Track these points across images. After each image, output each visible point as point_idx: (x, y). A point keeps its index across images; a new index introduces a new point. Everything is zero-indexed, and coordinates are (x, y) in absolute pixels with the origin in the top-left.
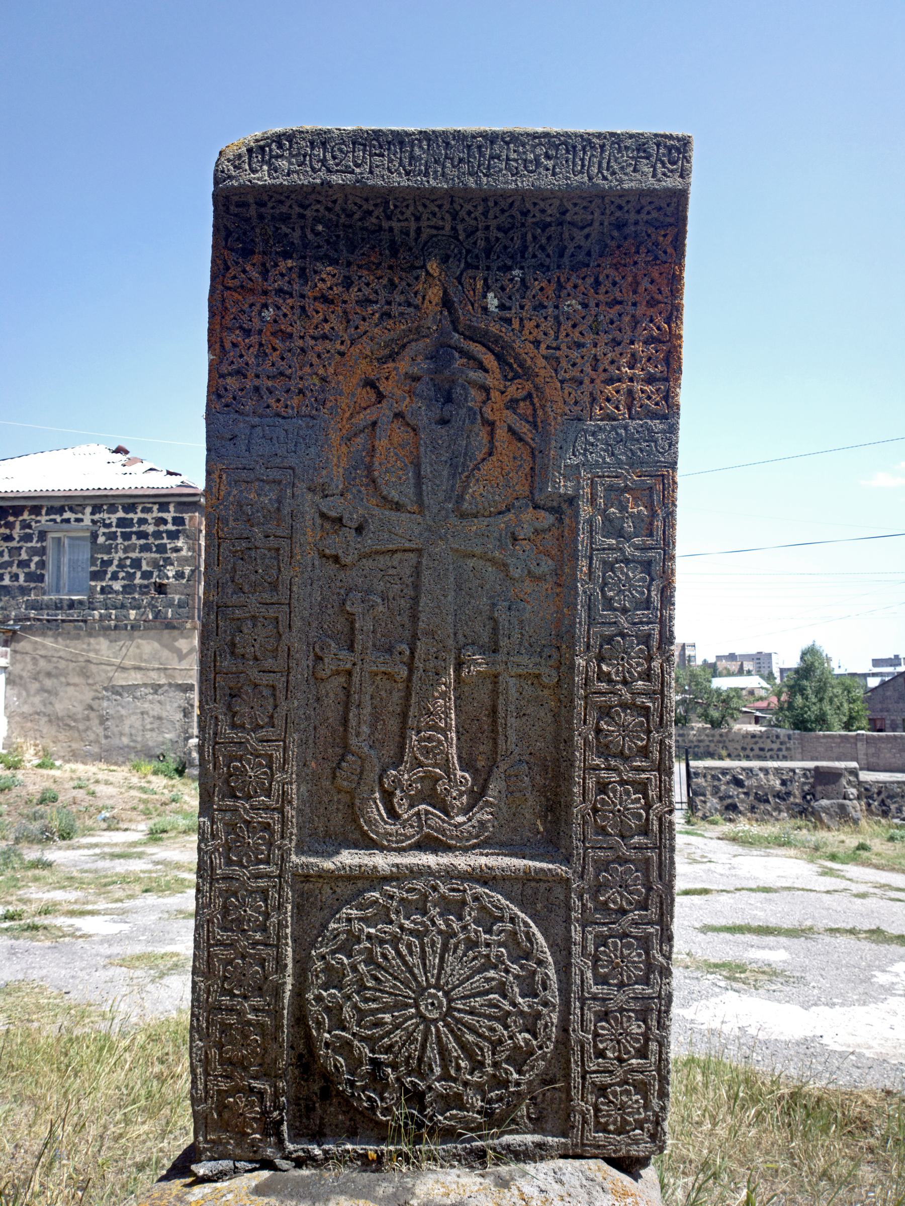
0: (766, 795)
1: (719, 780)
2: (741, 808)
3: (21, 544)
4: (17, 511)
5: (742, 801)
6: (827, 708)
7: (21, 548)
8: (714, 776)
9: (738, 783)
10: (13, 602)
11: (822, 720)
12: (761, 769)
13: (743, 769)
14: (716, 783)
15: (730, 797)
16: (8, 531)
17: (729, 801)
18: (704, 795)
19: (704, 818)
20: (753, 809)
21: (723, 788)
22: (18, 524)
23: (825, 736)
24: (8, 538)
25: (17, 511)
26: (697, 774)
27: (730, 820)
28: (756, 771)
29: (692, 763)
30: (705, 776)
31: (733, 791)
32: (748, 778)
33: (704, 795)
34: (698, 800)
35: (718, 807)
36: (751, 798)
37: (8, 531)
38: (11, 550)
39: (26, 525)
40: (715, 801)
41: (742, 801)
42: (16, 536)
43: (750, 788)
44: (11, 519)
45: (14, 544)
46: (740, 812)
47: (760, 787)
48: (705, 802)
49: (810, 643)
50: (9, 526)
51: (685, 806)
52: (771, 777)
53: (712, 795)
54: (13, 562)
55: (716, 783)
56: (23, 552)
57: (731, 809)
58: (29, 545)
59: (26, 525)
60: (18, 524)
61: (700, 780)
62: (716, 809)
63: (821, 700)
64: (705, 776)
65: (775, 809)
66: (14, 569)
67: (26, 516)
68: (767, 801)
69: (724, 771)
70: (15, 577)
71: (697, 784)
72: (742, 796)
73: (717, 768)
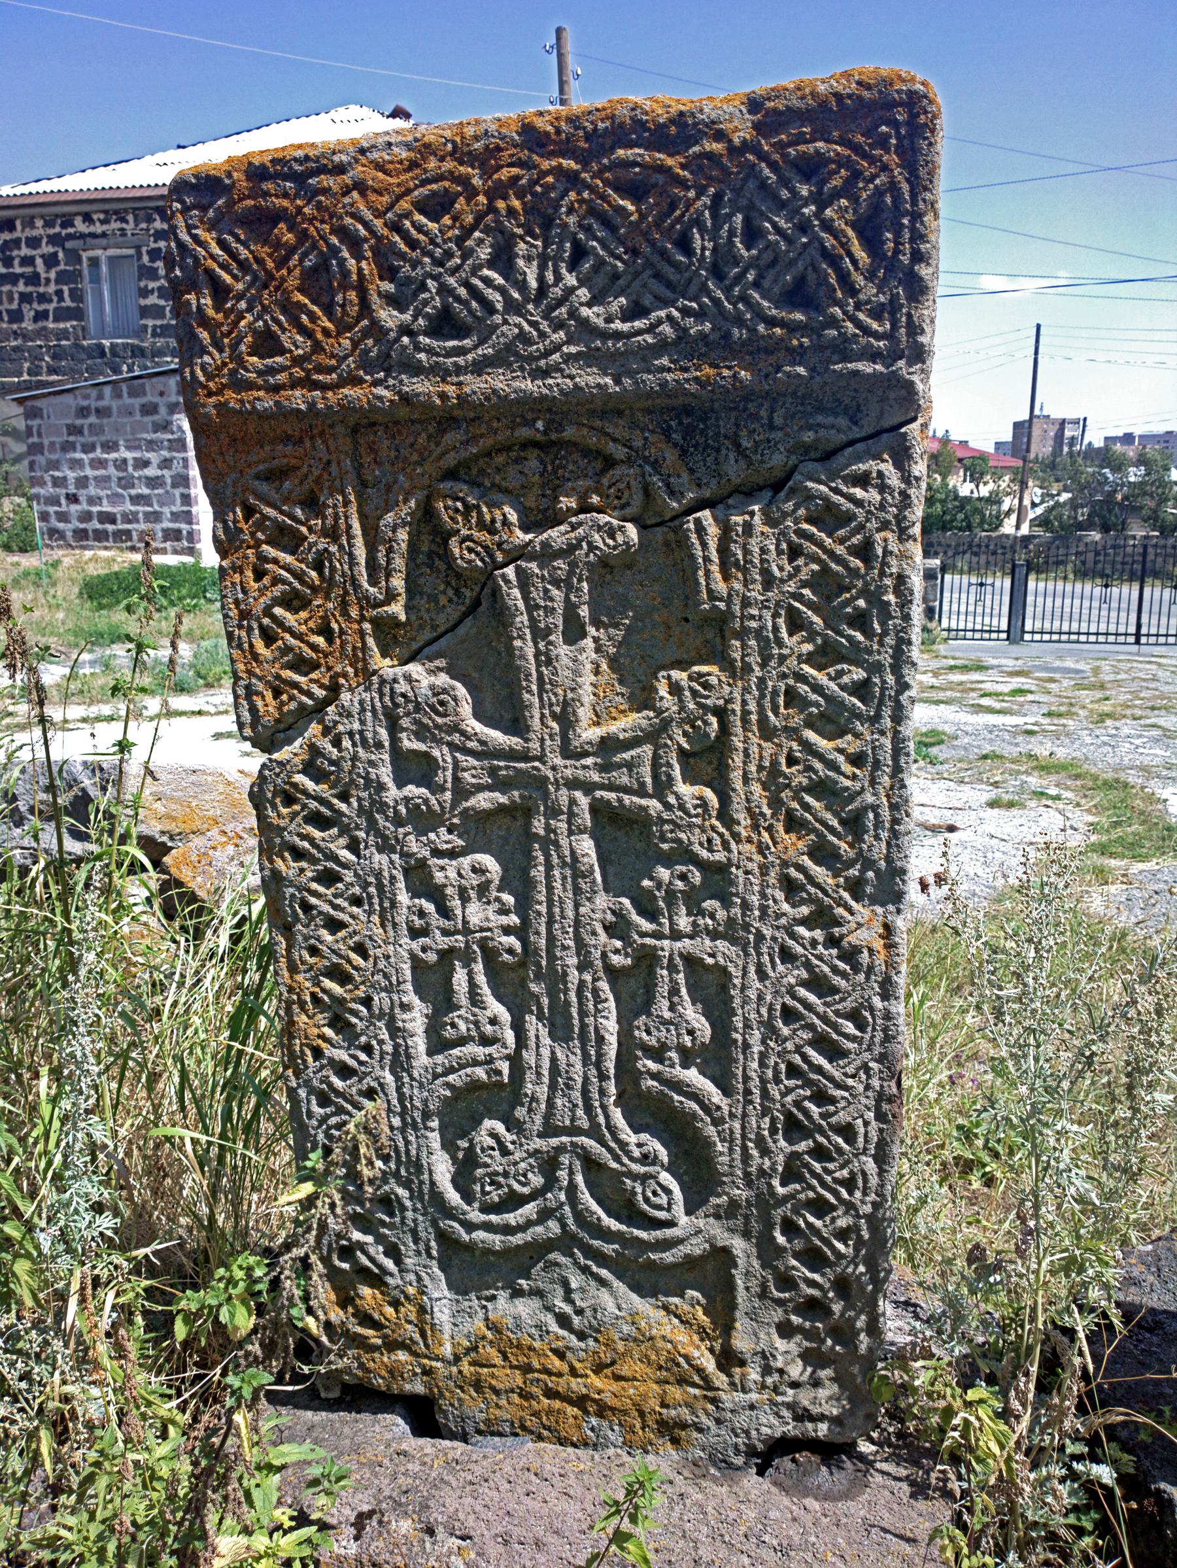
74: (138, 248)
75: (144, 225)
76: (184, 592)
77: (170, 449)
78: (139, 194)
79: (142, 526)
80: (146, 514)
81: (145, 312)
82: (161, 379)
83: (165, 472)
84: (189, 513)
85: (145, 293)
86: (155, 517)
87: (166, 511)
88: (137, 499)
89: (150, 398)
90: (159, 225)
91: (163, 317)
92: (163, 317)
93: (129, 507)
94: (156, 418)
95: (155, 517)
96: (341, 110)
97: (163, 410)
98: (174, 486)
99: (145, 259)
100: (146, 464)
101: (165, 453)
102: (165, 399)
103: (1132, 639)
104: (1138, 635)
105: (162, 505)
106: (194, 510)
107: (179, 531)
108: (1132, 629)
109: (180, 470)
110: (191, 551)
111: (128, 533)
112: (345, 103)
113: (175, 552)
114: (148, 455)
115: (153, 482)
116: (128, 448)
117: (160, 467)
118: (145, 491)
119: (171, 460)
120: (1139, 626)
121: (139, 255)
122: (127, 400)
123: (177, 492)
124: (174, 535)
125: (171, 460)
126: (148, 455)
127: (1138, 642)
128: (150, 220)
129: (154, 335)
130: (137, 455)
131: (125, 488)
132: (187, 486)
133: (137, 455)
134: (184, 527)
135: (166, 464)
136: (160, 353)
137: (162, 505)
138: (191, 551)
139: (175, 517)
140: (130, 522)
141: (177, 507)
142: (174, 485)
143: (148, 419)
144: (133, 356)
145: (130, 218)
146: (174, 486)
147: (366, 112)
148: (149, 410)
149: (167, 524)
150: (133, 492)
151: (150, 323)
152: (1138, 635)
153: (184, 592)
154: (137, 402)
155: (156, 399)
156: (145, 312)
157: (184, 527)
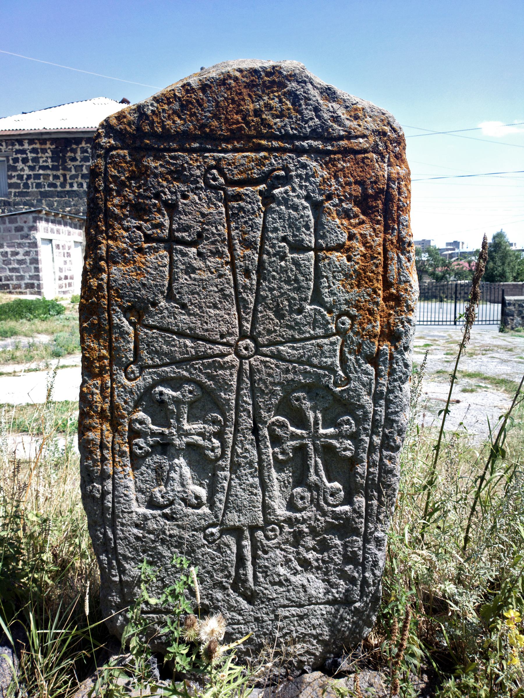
3: (82, 163)
4: (78, 141)
6: (507, 269)
7: (82, 166)
10: (81, 201)
11: (503, 276)
16: (73, 155)
18: (513, 316)
19: (512, 329)
22: (79, 150)
23: (503, 285)
24: (74, 159)
25: (78, 141)
26: (510, 304)
29: (507, 298)
33: (513, 316)
34: (509, 319)
37: (73, 155)
38: (76, 167)
39: (84, 151)
40: (519, 319)
42: (78, 158)
44: (74, 146)
45: (78, 163)
49: (499, 231)
50: (74, 151)
51: (499, 322)
53: (518, 316)
54: (78, 175)
56: (84, 168)
58: (88, 164)
59: (84, 151)
60: (79, 150)
61: (512, 308)
63: (503, 264)
64: (514, 305)
66: (80, 179)
67: (83, 145)
70: (80, 185)
74: (7, 157)
75: (10, 147)
76: (41, 311)
77: (29, 247)
78: (8, 133)
79: (15, 282)
80: (17, 277)
81: (11, 186)
82: (25, 215)
83: (27, 257)
84: (38, 276)
85: (10, 177)
86: (22, 278)
87: (27, 275)
88: (12, 270)
89: (20, 224)
90: (17, 147)
91: (20, 188)
92: (20, 188)
93: (8, 273)
94: (22, 233)
95: (22, 278)
96: (97, 99)
97: (26, 230)
98: (31, 263)
99: (11, 162)
100: (17, 254)
101: (27, 249)
102: (27, 224)
103: (453, 323)
104: (455, 322)
105: (25, 272)
106: (41, 274)
107: (33, 284)
108: (453, 319)
109: (34, 256)
110: (39, 293)
111: (8, 285)
112: (98, 96)
113: (31, 293)
114: (18, 250)
115: (20, 262)
116: (8, 246)
117: (24, 255)
118: (17, 266)
120: (455, 317)
121: (8, 161)
122: (8, 225)
123: (32, 266)
124: (32, 286)
126: (18, 250)
127: (455, 324)
128: (13, 145)
129: (15, 196)
130: (13, 249)
131: (6, 265)
132: (38, 263)
133: (13, 249)
134: (36, 282)
135: (27, 253)
136: (18, 204)
137: (25, 272)
138: (39, 293)
139: (31, 277)
140: (8, 280)
141: (33, 273)
142: (31, 263)
143: (19, 233)
144: (5, 205)
145: (4, 144)
146: (31, 263)
147: (108, 100)
148: (19, 229)
149: (27, 281)
150: (10, 267)
151: (13, 190)
152: (455, 322)
153: (41, 311)
154: (13, 226)
155: (23, 224)
156: (11, 186)
157: (36, 282)
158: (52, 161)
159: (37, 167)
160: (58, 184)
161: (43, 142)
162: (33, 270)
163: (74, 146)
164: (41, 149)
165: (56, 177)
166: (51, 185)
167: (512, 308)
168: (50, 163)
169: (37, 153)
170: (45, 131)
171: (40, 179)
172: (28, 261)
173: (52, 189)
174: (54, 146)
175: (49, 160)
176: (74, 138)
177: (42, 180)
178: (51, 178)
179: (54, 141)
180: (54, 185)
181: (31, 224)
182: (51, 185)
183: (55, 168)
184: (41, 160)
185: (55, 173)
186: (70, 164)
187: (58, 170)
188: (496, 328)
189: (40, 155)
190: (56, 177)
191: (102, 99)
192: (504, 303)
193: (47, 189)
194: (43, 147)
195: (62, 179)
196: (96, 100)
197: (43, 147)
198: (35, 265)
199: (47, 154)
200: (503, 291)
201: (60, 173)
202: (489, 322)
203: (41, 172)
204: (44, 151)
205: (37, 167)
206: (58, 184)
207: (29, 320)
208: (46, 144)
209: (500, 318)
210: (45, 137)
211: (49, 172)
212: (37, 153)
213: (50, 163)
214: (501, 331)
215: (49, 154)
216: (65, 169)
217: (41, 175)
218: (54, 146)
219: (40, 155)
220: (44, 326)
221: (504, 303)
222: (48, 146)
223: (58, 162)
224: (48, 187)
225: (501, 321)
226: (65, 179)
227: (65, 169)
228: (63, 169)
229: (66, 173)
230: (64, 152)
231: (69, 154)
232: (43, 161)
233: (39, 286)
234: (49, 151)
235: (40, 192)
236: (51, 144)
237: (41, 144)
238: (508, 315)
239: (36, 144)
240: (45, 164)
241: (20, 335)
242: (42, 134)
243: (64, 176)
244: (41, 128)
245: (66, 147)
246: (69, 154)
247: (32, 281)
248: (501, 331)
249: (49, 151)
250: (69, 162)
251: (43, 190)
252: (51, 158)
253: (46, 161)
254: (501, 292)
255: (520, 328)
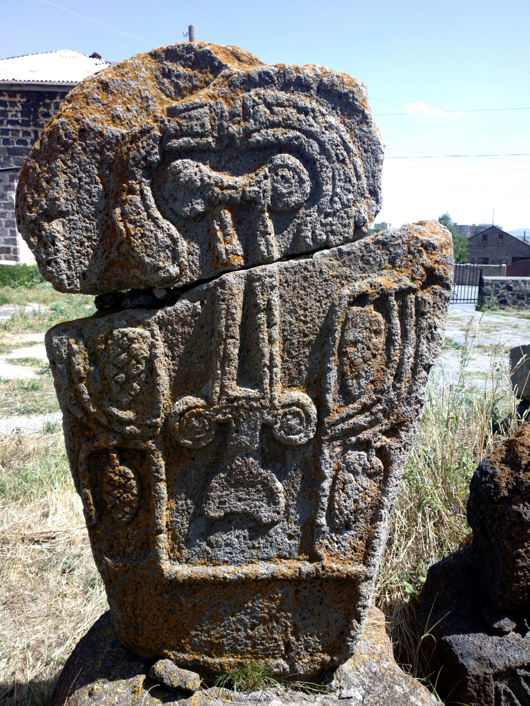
0: (523, 295)
1: (499, 287)
2: (509, 302)
4: (52, 95)
5: (510, 298)
8: (496, 284)
9: (509, 288)
12: (522, 281)
13: (513, 281)
14: (497, 289)
15: (504, 296)
16: (45, 110)
17: (503, 298)
18: (490, 295)
19: (489, 308)
20: (514, 303)
21: (500, 292)
22: (52, 105)
26: (487, 284)
27: (503, 309)
28: (520, 282)
29: (485, 278)
30: (491, 285)
31: (506, 293)
32: (515, 286)
33: (490, 295)
34: (486, 298)
35: (496, 301)
36: (515, 297)
37: (45, 110)
40: (495, 298)
41: (510, 298)
43: (515, 291)
44: (48, 101)
46: (508, 305)
47: (521, 291)
48: (489, 299)
50: (47, 106)
51: (476, 301)
52: (527, 285)
53: (495, 295)
55: (497, 289)
57: (503, 303)
60: (52, 105)
61: (489, 287)
62: (495, 303)
64: (491, 285)
65: (526, 303)
68: (523, 298)
69: (502, 282)
71: (487, 289)
72: (510, 296)
73: (498, 280)
77: (5, 208)
84: (15, 240)
96: (62, 51)
107: (9, 249)
110: (16, 259)
113: (7, 259)
119: (5, 213)
123: (8, 229)
125: (5, 213)
134: (12, 247)
141: (8, 236)
147: (74, 54)
157: (12, 247)
158: (22, 116)
159: (5, 122)
160: (29, 141)
161: (13, 94)
162: (9, 234)
163: (48, 101)
164: (10, 102)
165: (26, 133)
166: (20, 142)
167: (489, 287)
168: (19, 118)
169: (6, 106)
170: (14, 82)
171: (8, 134)
172: (4, 224)
173: (21, 146)
174: (24, 100)
175: (19, 115)
176: (48, 93)
177: (10, 136)
178: (21, 134)
179: (24, 94)
180: (24, 143)
181: (7, 183)
182: (20, 142)
183: (25, 124)
184: (10, 114)
185: (25, 129)
186: (42, 120)
187: (30, 126)
188: (473, 306)
189: (8, 108)
190: (26, 133)
191: (69, 53)
192: (481, 284)
193: (16, 145)
194: (12, 99)
195: (33, 136)
196: (63, 52)
197: (12, 99)
198: (11, 228)
199: (16, 108)
200: (481, 271)
201: (30, 129)
202: (467, 300)
203: (9, 127)
204: (13, 104)
205: (5, 122)
206: (29, 141)
207: (13, 288)
208: (16, 97)
209: (477, 297)
210: (15, 89)
211: (18, 127)
212: (6, 106)
213: (19, 118)
214: (478, 309)
215: (19, 108)
216: (37, 125)
217: (9, 130)
218: (24, 100)
219: (8, 108)
220: (31, 294)
221: (481, 284)
222: (18, 98)
223: (29, 118)
224: (17, 143)
225: (478, 299)
226: (36, 137)
227: (37, 125)
228: (34, 125)
229: (38, 129)
230: (36, 106)
231: (41, 109)
232: (12, 116)
233: (16, 251)
234: (19, 104)
235: (8, 148)
236: (22, 97)
237: (10, 96)
238: (485, 294)
239: (4, 96)
240: (14, 118)
241: (12, 303)
242: (12, 85)
243: (36, 132)
244: (10, 79)
245: (39, 101)
246: (41, 109)
247: (8, 246)
248: (478, 309)
249: (19, 104)
250: (42, 118)
251: (11, 146)
252: (22, 112)
253: (15, 116)
254: (479, 272)
255: (495, 307)
